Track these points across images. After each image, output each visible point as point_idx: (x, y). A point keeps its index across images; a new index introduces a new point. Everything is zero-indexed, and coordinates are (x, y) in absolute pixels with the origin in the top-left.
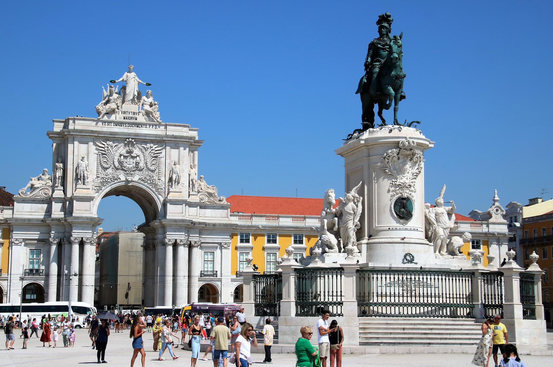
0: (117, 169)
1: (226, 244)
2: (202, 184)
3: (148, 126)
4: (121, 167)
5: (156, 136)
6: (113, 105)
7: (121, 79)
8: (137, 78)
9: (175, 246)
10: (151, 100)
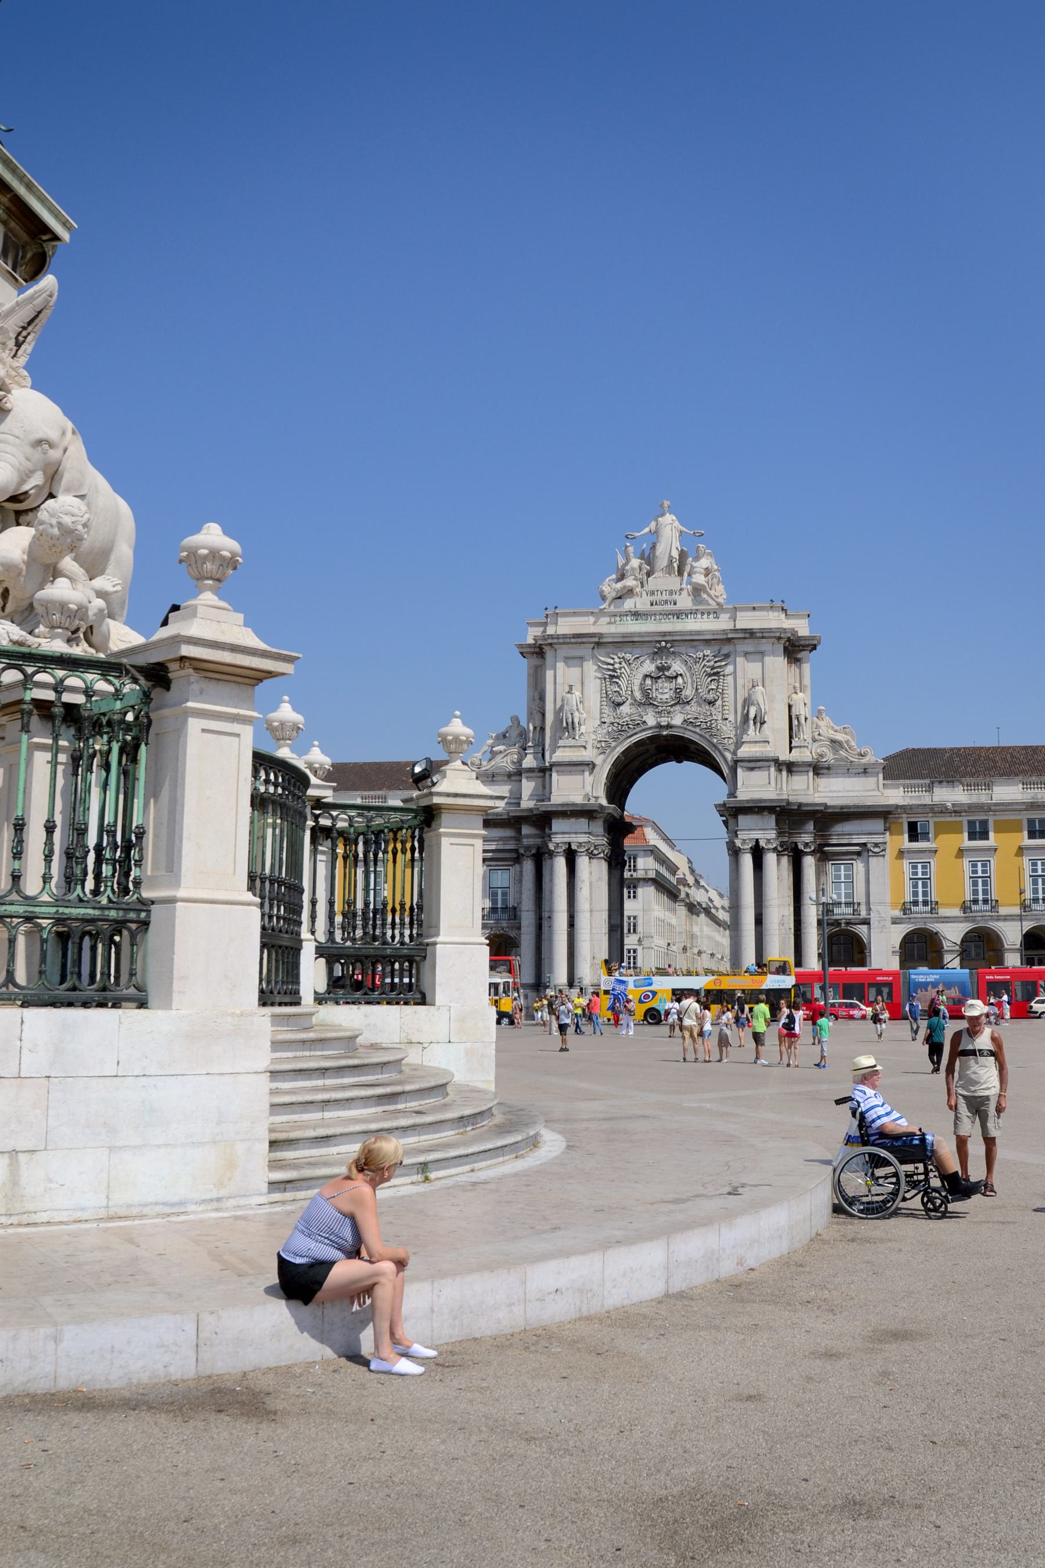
0: (640, 704)
1: (876, 845)
2: (821, 723)
3: (699, 616)
4: (648, 701)
5: (714, 632)
6: (629, 582)
7: (647, 530)
8: (677, 523)
9: (758, 853)
10: (704, 562)
